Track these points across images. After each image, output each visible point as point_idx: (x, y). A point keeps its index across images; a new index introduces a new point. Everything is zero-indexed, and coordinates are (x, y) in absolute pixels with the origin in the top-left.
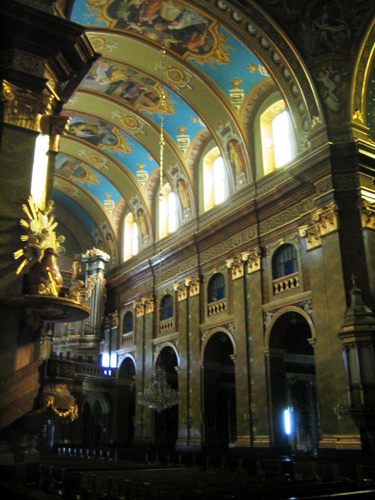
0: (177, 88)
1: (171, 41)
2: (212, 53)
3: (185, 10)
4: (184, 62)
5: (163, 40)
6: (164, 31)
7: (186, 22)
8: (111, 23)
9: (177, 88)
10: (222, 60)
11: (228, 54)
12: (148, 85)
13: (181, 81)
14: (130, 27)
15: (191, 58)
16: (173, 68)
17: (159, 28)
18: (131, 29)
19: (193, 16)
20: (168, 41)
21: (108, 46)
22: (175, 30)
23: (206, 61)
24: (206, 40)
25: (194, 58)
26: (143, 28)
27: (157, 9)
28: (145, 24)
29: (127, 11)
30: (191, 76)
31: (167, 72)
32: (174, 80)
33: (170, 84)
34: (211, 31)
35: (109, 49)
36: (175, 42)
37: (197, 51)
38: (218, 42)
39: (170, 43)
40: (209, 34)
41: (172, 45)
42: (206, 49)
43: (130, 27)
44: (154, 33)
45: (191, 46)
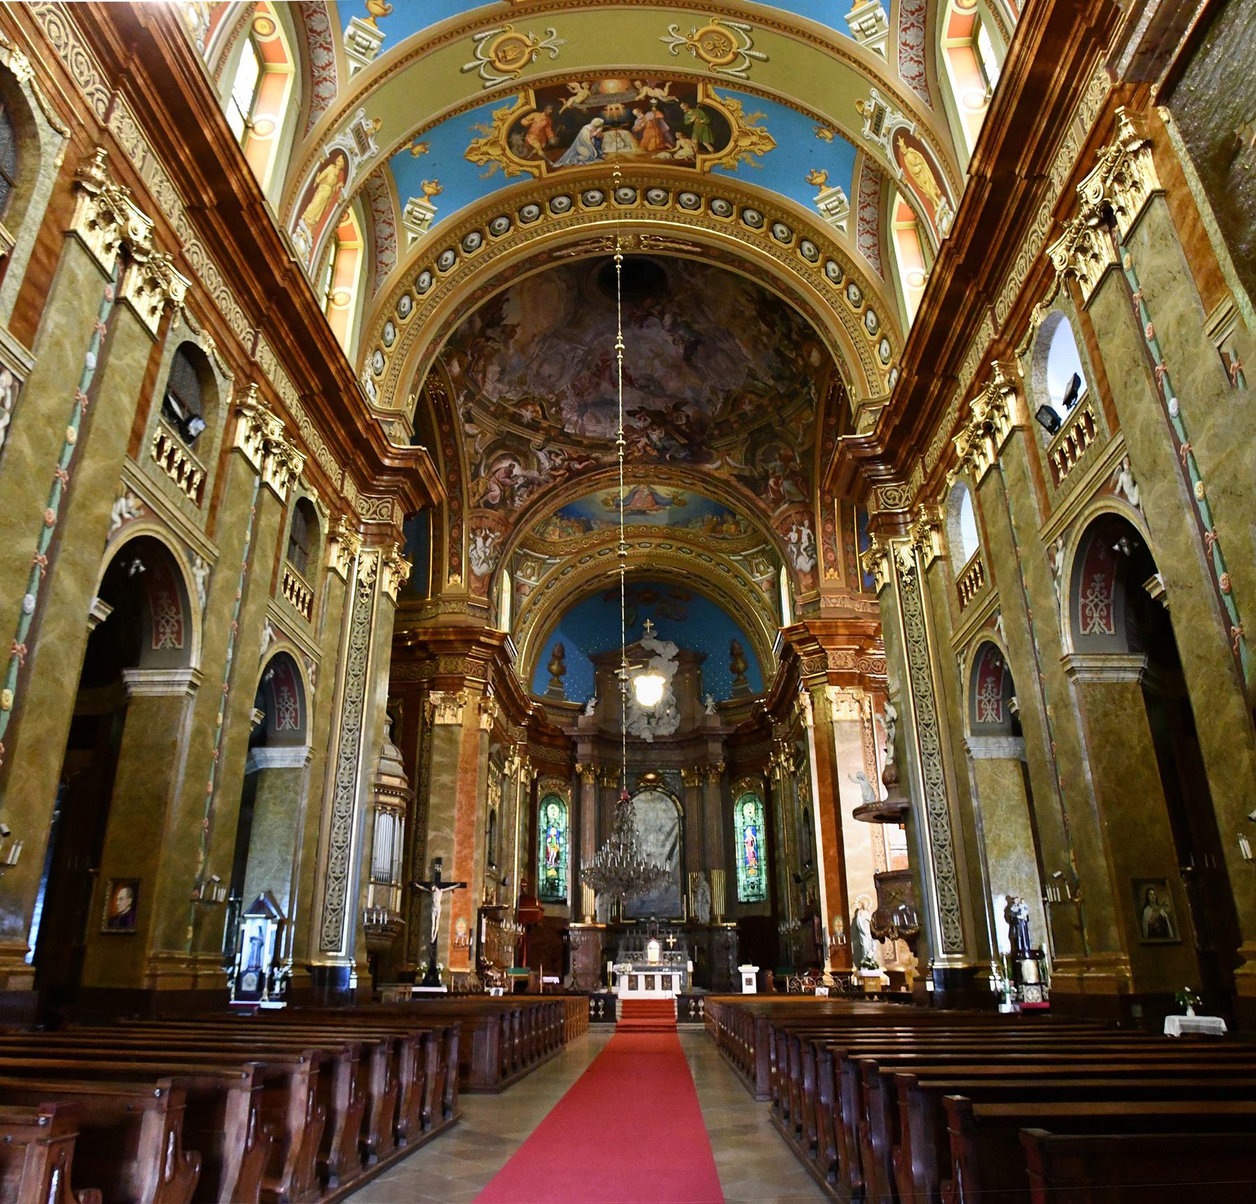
2: (503, 142)
3: (599, 157)
4: (524, 86)
6: (603, 108)
7: (583, 144)
8: (708, 96)
11: (481, 163)
14: (666, 89)
15: (521, 101)
16: (530, 60)
17: (615, 109)
18: (661, 86)
20: (580, 95)
21: (684, 40)
22: (589, 122)
23: (495, 124)
24: (531, 148)
25: (514, 108)
26: (641, 96)
27: (643, 141)
28: (645, 105)
30: (488, 84)
31: (529, 43)
35: (677, 30)
36: (569, 103)
37: (524, 122)
38: (512, 161)
39: (575, 94)
40: (536, 157)
41: (569, 94)
42: (517, 138)
43: (666, 89)
44: (615, 95)
45: (539, 119)
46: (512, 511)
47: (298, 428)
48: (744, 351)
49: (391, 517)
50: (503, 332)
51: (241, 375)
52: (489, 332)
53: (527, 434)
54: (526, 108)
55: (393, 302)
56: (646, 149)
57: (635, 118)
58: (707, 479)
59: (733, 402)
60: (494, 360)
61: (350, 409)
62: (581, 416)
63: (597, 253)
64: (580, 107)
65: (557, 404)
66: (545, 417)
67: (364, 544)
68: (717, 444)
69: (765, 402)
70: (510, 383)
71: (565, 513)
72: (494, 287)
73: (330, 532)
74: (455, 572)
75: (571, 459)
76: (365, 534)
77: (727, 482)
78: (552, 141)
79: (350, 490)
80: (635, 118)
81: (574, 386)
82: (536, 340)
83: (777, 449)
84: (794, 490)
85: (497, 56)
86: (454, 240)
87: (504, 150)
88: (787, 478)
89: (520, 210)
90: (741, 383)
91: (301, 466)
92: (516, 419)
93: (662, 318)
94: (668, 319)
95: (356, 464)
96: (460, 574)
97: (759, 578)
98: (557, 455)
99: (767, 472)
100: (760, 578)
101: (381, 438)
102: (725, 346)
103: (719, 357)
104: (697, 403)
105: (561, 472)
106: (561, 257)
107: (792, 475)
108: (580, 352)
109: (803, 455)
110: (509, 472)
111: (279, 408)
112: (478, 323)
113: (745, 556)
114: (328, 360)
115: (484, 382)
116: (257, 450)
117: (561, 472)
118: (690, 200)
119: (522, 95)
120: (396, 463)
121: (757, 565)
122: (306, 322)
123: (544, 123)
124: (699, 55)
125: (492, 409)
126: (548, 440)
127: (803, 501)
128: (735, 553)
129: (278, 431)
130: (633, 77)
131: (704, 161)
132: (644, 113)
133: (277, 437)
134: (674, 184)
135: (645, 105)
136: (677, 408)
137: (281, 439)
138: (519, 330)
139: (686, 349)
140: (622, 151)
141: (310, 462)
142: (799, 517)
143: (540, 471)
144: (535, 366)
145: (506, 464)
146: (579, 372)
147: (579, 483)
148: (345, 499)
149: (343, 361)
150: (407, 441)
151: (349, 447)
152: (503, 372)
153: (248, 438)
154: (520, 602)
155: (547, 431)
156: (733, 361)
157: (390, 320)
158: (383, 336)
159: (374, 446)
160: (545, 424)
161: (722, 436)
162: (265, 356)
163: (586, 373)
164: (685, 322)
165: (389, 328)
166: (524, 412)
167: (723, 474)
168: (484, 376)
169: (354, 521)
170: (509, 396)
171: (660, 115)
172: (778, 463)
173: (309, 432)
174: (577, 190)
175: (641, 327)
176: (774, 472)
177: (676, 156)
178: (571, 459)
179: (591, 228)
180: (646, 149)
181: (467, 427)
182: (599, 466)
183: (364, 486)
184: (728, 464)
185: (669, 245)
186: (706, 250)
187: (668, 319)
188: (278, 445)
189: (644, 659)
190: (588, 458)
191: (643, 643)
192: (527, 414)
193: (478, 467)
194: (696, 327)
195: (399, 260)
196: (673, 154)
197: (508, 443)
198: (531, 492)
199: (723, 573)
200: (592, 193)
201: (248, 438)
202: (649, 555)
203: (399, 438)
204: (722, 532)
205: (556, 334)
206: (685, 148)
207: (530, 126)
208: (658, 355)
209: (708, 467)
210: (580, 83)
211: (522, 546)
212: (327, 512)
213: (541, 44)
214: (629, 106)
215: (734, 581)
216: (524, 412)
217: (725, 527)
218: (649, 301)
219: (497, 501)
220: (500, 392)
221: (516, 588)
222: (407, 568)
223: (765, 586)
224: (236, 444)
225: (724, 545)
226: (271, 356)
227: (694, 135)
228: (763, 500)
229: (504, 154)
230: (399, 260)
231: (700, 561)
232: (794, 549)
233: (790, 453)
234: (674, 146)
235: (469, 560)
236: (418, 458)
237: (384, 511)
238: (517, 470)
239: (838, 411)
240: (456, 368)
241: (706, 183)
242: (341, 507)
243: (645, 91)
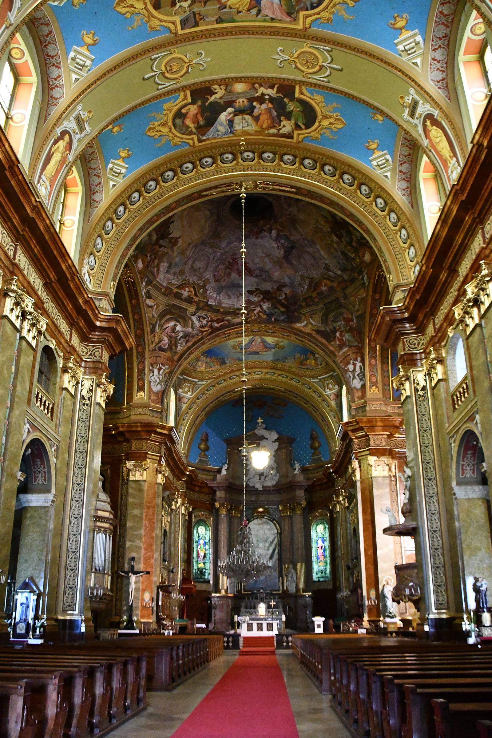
0: (157, 56)
1: (217, 96)
2: (170, 124)
3: (231, 132)
4: (184, 88)
5: (225, 90)
6: (234, 101)
7: (221, 124)
9: (157, 56)
10: (154, 128)
11: (156, 137)
12: (188, 13)
13: (163, 69)
14: (275, 89)
16: (187, 72)
17: (241, 102)
18: (272, 87)
19: (219, 133)
20: (220, 93)
21: (287, 57)
23: (165, 112)
24: (188, 127)
26: (259, 94)
27: (260, 122)
28: (261, 99)
29: (292, 111)
31: (187, 61)
32: (172, 59)
33: (170, 50)
34: (192, 136)
36: (212, 99)
37: (184, 111)
39: (216, 93)
40: (191, 133)
41: (213, 93)
42: (178, 121)
43: (275, 89)
44: (242, 93)
45: (193, 109)
46: (176, 353)
47: (43, 303)
48: (322, 252)
49: (101, 357)
50: (170, 242)
51: (7, 271)
52: (161, 242)
53: (185, 305)
54: (185, 102)
55: (101, 224)
56: (261, 127)
57: (255, 107)
58: (298, 333)
59: (315, 285)
60: (165, 259)
61: (74, 290)
62: (219, 294)
63: (230, 193)
64: (219, 101)
65: (204, 287)
66: (196, 295)
67: (85, 373)
68: (304, 311)
69: (335, 284)
70: (174, 274)
71: (208, 353)
72: (165, 214)
73: (63, 367)
74: (140, 390)
75: (212, 321)
76: (85, 368)
77: (309, 335)
78: (202, 123)
79: (75, 341)
80: (255, 107)
81: (214, 276)
82: (191, 246)
83: (342, 314)
84: (351, 339)
85: (166, 69)
86: (139, 185)
87: (170, 129)
88: (348, 331)
89: (181, 167)
90: (320, 273)
91: (45, 326)
92: (178, 296)
93: (270, 233)
94: (274, 233)
95: (78, 324)
96: (144, 391)
97: (328, 392)
98: (204, 318)
99: (335, 328)
100: (330, 392)
101: (94, 308)
102: (310, 250)
103: (307, 257)
104: (292, 285)
105: (206, 329)
106: (207, 195)
107: (351, 330)
108: (218, 254)
109: (357, 317)
110: (174, 329)
111: (31, 291)
112: (155, 237)
113: (320, 379)
114: (60, 261)
115: (158, 273)
116: (18, 317)
117: (206, 329)
118: (289, 159)
119: (182, 94)
120: (104, 324)
121: (328, 384)
122: (47, 238)
123: (196, 111)
124: (296, 67)
125: (163, 290)
126: (198, 309)
127: (357, 346)
128: (313, 377)
129: (30, 305)
130: (253, 82)
131: (299, 135)
132: (261, 104)
133: (30, 309)
134: (279, 150)
135: (261, 99)
136: (280, 289)
137: (32, 310)
138: (180, 240)
139: (285, 251)
140: (246, 128)
141: (50, 323)
142: (354, 355)
143: (193, 328)
144: (190, 263)
145: (172, 324)
146: (218, 266)
147: (218, 336)
148: (72, 347)
149: (70, 262)
150: (111, 310)
151: (74, 315)
152: (169, 267)
153: (12, 310)
154: (181, 408)
155: (197, 303)
156: (315, 259)
157: (99, 236)
158: (95, 246)
159: (90, 313)
160: (196, 299)
161: (308, 306)
162: (22, 260)
163: (222, 267)
164: (285, 235)
165: (99, 241)
166: (183, 292)
167: (308, 330)
168: (158, 270)
169: (78, 360)
170: (173, 282)
171: (270, 106)
172: (343, 322)
173: (50, 305)
174: (216, 153)
175: (257, 238)
176: (340, 328)
177: (281, 132)
178: (212, 321)
179: (226, 177)
180: (261, 127)
181: (148, 300)
182: (230, 325)
183: (84, 339)
184: (311, 323)
185: (276, 187)
186: (299, 191)
187: (274, 233)
188: (31, 314)
189: (257, 441)
190: (223, 320)
191: (256, 432)
192: (185, 293)
193: (154, 326)
194: (292, 238)
195: (105, 198)
196: (279, 130)
197: (173, 311)
198: (188, 341)
199: (306, 389)
200: (227, 155)
201: (12, 310)
202: (261, 379)
203: (105, 309)
204: (306, 365)
205: (203, 243)
206: (287, 126)
207: (187, 113)
208: (268, 255)
209: (298, 325)
210: (220, 86)
211: (182, 374)
212: (62, 354)
213: (195, 61)
214: (251, 100)
215: (313, 394)
216: (183, 292)
217: (308, 362)
218: (262, 222)
219: (166, 347)
220: (168, 279)
221: (179, 399)
222: (111, 388)
223: (332, 397)
224: (4, 314)
225: (308, 373)
226: (25, 259)
227: (293, 119)
228: (332, 345)
229: (170, 131)
230: (105, 198)
231: (292, 382)
232: (351, 375)
233: (350, 316)
234: (280, 125)
235: (150, 383)
236: (118, 322)
237: (96, 354)
238: (179, 328)
239: (381, 291)
240: (140, 265)
241: (298, 148)
242: (70, 351)
243: (262, 90)
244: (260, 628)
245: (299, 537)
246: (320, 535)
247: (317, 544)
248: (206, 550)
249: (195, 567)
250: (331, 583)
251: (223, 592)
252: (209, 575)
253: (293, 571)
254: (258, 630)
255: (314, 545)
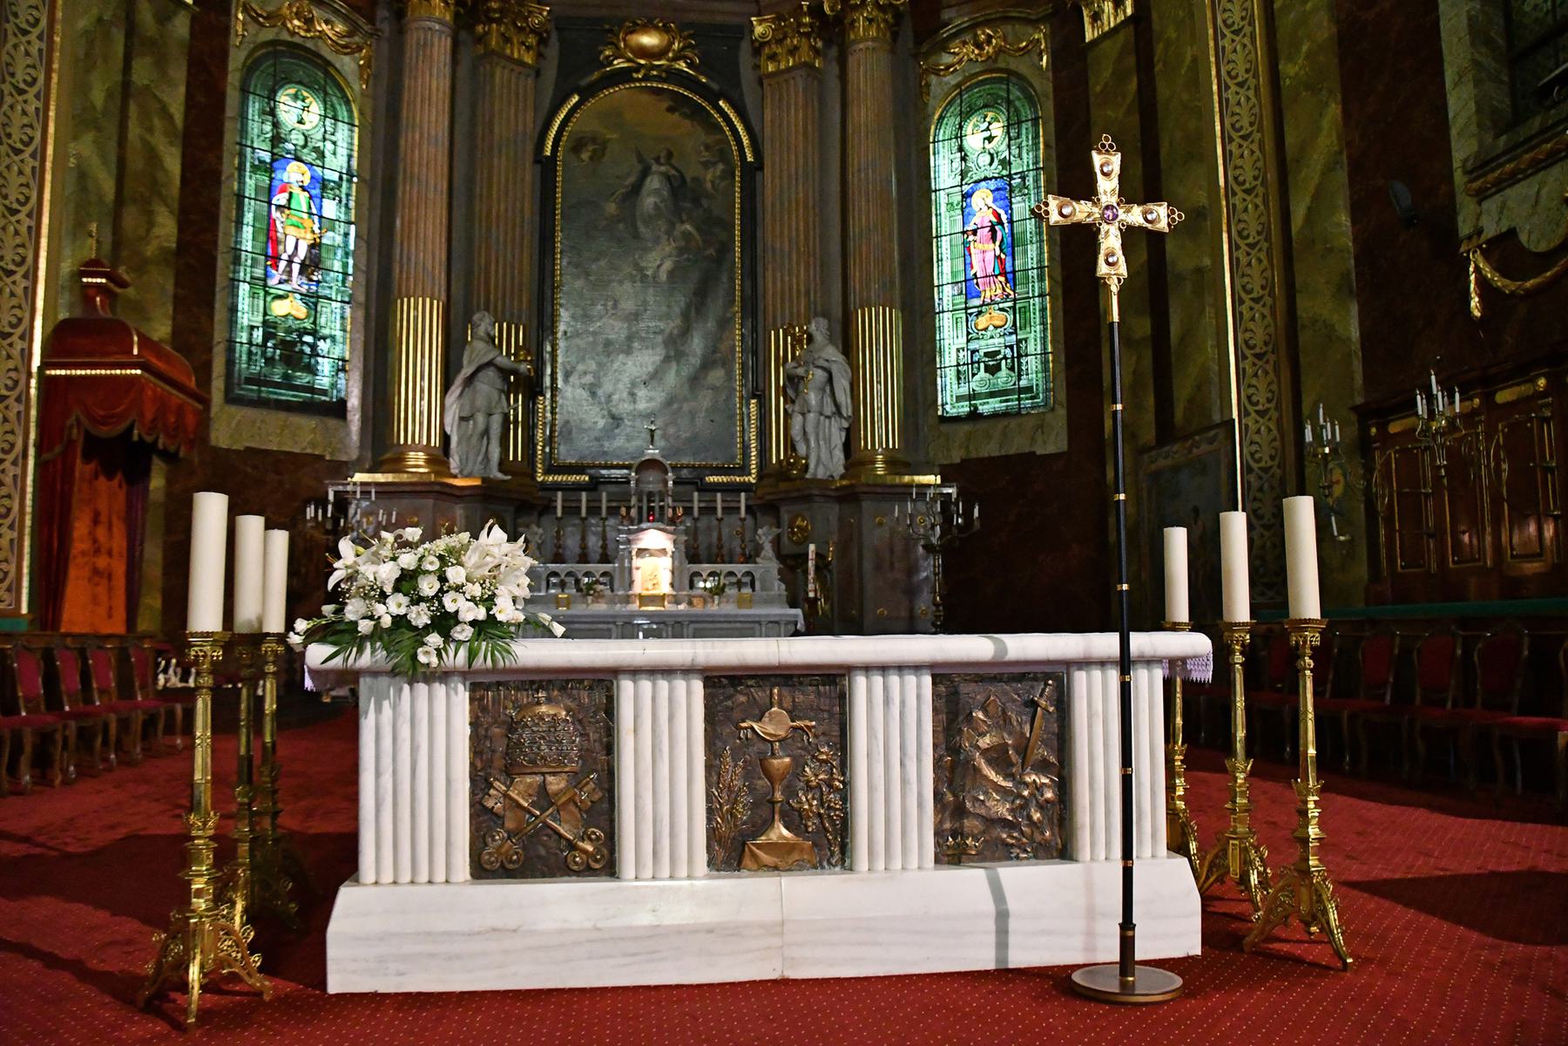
244: (779, 805)
245: (871, 157)
246: (981, 164)
247: (966, 213)
248: (327, 224)
249: (248, 312)
250: (1060, 419)
251: (417, 461)
252: (334, 366)
253: (833, 354)
254: (731, 849)
255: (946, 221)
